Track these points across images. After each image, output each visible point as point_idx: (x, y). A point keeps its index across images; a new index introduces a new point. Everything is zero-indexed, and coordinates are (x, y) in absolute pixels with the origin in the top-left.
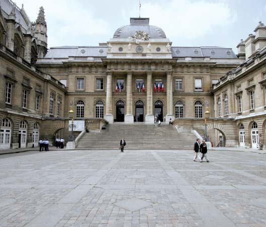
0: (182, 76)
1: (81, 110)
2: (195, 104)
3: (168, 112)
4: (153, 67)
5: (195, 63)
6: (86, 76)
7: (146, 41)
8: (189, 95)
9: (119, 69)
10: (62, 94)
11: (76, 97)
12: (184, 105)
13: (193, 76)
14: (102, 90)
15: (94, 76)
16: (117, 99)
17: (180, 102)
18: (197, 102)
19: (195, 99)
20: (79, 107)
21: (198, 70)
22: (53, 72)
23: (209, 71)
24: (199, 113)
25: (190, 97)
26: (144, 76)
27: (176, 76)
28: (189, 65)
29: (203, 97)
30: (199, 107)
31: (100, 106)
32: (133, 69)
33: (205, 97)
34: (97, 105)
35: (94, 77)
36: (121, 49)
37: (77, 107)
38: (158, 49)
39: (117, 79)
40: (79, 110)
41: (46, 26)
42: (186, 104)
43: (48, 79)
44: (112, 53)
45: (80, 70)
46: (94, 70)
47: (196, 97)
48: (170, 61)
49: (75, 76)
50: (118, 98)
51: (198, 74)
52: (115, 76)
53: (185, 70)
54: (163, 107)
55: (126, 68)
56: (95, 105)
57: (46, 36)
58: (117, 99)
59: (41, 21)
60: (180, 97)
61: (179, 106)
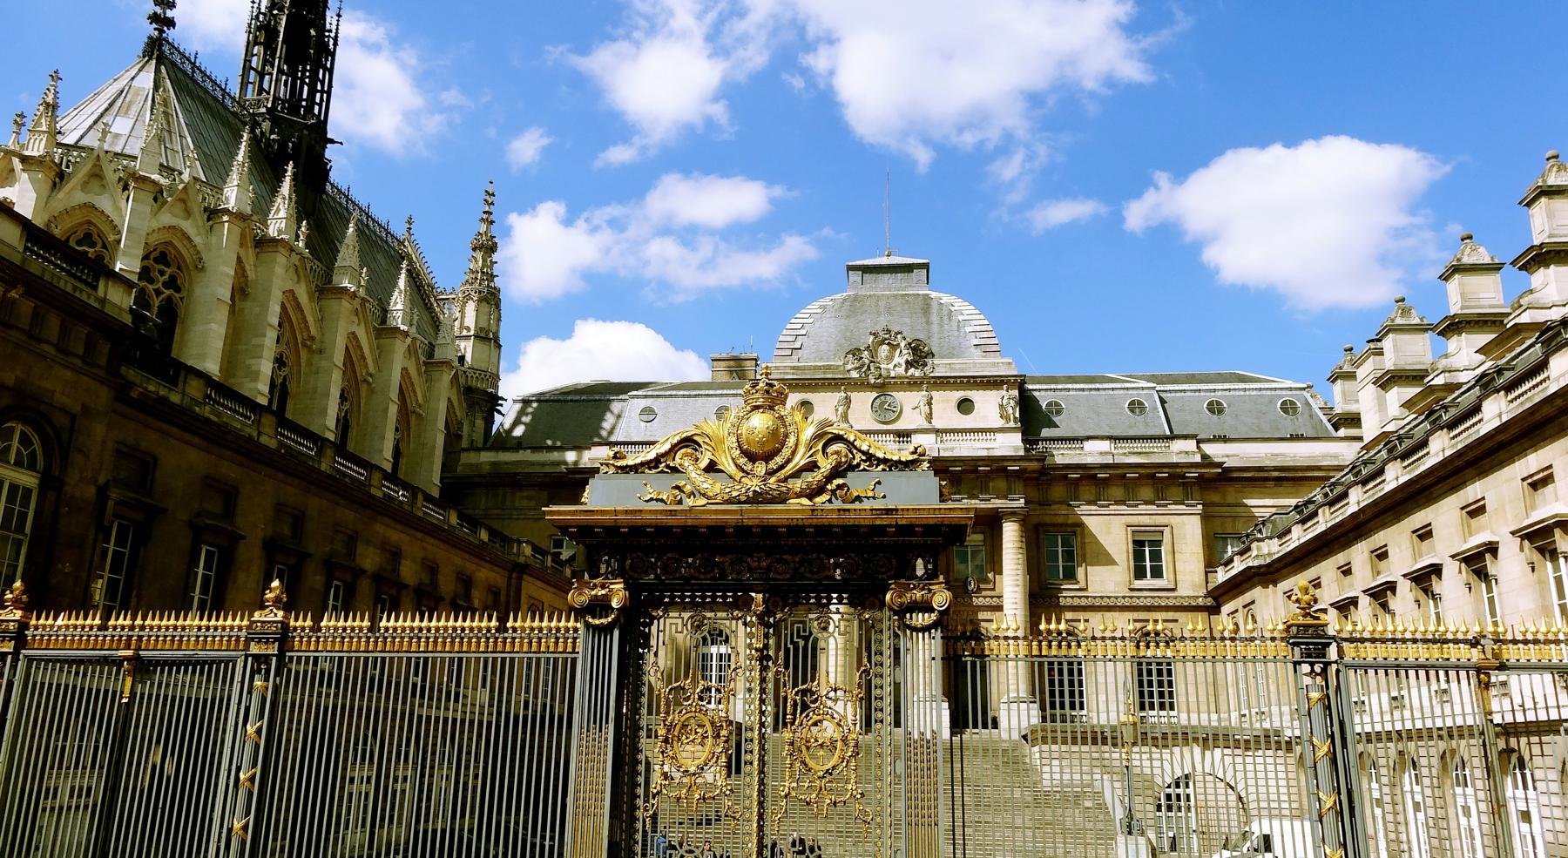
24: (1153, 686)
27: (1048, 520)
38: (965, 406)
41: (498, 305)
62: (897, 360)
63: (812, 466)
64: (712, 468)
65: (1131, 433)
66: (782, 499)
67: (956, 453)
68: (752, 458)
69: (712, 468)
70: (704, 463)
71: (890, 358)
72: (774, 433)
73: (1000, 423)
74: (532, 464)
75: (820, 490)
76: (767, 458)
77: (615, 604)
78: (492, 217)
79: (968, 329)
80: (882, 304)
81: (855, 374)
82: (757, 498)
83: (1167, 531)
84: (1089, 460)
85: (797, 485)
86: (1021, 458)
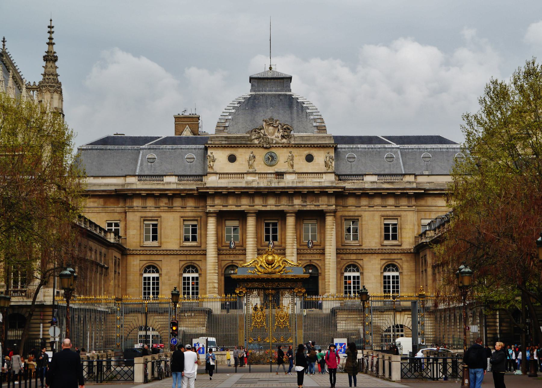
0: (357, 214)
1: (153, 284)
2: (385, 270)
3: (327, 291)
4: (297, 202)
5: (384, 189)
6: (163, 215)
7: (284, 141)
8: (371, 252)
9: (232, 205)
10: (118, 256)
11: (142, 257)
12: (362, 273)
13: (380, 213)
14: (194, 244)
15: (177, 215)
16: (227, 262)
17: (355, 267)
18: (388, 266)
19: (384, 262)
20: (149, 278)
21: (391, 201)
22: (92, 205)
23: (413, 202)
25: (374, 256)
26: (282, 215)
27: (346, 214)
28: (371, 193)
29: (399, 256)
30: (393, 277)
31: (191, 275)
32: (259, 204)
33: (404, 258)
34: (186, 275)
35: (178, 218)
36: (232, 159)
37: (145, 278)
38: (310, 158)
39: (225, 220)
40: (149, 284)
42: (365, 274)
43: (112, 241)
44: (217, 173)
45: (150, 203)
46: (178, 203)
47: (387, 256)
48: (331, 191)
49: (139, 214)
50: (228, 260)
51: (390, 210)
52: (222, 216)
53: (364, 202)
54: (320, 277)
55: (245, 204)
56: (181, 275)
57: (64, 115)
58: (227, 262)
59: (51, 83)
60: (353, 257)
61: (352, 274)
62: (276, 134)
63: (280, 266)
64: (261, 266)
65: (387, 172)
66: (275, 273)
67: (305, 185)
68: (269, 265)
69: (261, 266)
70: (259, 265)
71: (273, 134)
72: (272, 260)
73: (324, 169)
74: (94, 185)
75: (281, 271)
76: (271, 264)
77: (244, 292)
78: (53, 41)
79: (312, 117)
80: (269, 101)
81: (256, 142)
82: (269, 273)
83: (399, 218)
84: (367, 186)
85: (277, 270)
86: (335, 188)
